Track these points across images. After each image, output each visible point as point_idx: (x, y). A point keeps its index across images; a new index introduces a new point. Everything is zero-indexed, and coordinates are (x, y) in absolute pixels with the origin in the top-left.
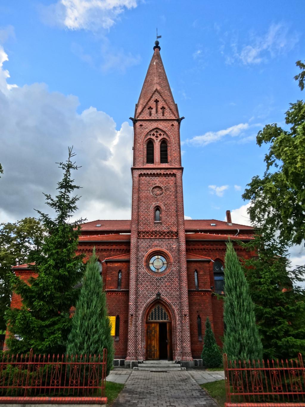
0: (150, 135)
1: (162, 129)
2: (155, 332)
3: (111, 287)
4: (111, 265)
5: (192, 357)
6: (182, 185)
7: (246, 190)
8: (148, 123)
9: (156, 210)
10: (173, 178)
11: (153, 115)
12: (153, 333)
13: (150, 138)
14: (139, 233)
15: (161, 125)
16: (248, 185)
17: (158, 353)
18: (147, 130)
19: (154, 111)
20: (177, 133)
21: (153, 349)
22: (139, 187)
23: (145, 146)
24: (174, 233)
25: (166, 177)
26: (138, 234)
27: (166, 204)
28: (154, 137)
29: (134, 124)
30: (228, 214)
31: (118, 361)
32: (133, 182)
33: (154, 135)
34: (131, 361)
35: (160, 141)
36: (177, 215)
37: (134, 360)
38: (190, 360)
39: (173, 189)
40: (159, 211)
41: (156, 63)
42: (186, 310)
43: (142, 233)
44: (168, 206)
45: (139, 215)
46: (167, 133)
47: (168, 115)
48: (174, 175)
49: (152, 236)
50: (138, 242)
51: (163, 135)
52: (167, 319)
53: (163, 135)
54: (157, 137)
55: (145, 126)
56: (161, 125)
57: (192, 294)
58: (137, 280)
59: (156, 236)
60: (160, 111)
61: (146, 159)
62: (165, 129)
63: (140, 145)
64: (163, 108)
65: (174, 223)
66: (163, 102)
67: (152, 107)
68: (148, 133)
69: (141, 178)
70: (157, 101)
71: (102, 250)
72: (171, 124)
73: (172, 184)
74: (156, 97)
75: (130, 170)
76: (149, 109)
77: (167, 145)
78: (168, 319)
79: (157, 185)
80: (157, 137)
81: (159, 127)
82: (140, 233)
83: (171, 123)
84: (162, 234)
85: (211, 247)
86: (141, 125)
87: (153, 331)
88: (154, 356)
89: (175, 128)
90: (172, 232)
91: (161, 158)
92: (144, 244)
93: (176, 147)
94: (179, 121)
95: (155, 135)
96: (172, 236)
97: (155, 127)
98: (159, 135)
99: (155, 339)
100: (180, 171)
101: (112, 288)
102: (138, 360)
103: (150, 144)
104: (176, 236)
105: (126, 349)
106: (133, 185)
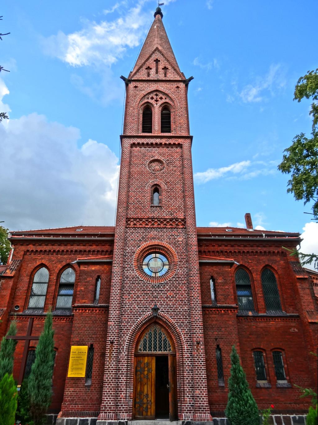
0: (148, 98)
1: (164, 91)
2: (149, 371)
3: (84, 301)
4: (86, 269)
5: (211, 413)
6: (191, 157)
7: (285, 157)
8: (146, 84)
9: (154, 192)
10: (178, 150)
11: (152, 75)
12: (146, 373)
13: (148, 102)
14: (128, 219)
15: (162, 87)
16: (287, 150)
17: (153, 407)
18: (144, 93)
19: (153, 72)
20: (183, 99)
21: (145, 401)
22: (130, 160)
23: (141, 112)
24: (180, 220)
25: (168, 148)
26: (127, 222)
27: (168, 182)
28: (153, 100)
29: (127, 85)
30: (248, 217)
31: (87, 420)
32: (122, 153)
33: (152, 98)
34: (107, 421)
35: (161, 106)
36: (184, 197)
37: (112, 419)
38: (208, 420)
39: (178, 163)
40: (159, 193)
41: (158, 26)
42: (199, 334)
43: (132, 220)
44: (171, 185)
45: (129, 196)
46: (170, 95)
47: (171, 76)
48: (180, 145)
49: (147, 224)
50: (126, 232)
51: (166, 98)
52: (168, 349)
53: (166, 98)
54: (157, 101)
55: (141, 88)
56: (161, 87)
57: (207, 312)
58: (122, 288)
59: (153, 224)
60: (161, 71)
61: (141, 126)
62: (167, 92)
63: (134, 109)
64: (165, 68)
65: (179, 207)
66: (166, 61)
67: (151, 67)
68: (145, 96)
69: (134, 148)
70: (157, 61)
71: (76, 251)
72: (176, 86)
73: (177, 156)
74: (157, 56)
75: (119, 137)
76: (146, 69)
77: (170, 111)
78: (170, 350)
79: (156, 158)
80: (157, 101)
81: (160, 90)
82: (129, 220)
83: (175, 85)
84: (162, 222)
85: (232, 249)
86: (136, 87)
87: (146, 369)
88: (147, 412)
89: (180, 91)
90: (177, 219)
91: (162, 127)
92: (135, 235)
93: (182, 112)
94: (186, 82)
95: (154, 98)
96: (177, 225)
97: (154, 89)
98: (160, 98)
99: (149, 383)
100: (188, 141)
101: (84, 303)
102: (119, 419)
103: (147, 111)
104: (183, 225)
105: (100, 401)
106: (122, 157)
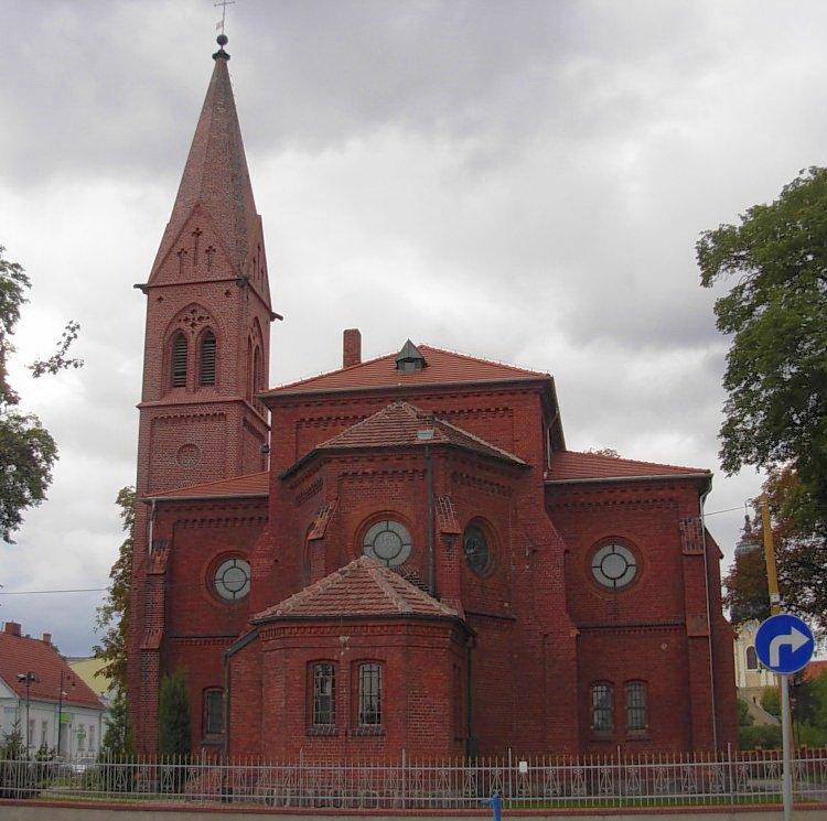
60: (202, 256)
64: (210, 250)
70: (198, 234)
103: (181, 338)
